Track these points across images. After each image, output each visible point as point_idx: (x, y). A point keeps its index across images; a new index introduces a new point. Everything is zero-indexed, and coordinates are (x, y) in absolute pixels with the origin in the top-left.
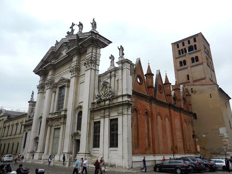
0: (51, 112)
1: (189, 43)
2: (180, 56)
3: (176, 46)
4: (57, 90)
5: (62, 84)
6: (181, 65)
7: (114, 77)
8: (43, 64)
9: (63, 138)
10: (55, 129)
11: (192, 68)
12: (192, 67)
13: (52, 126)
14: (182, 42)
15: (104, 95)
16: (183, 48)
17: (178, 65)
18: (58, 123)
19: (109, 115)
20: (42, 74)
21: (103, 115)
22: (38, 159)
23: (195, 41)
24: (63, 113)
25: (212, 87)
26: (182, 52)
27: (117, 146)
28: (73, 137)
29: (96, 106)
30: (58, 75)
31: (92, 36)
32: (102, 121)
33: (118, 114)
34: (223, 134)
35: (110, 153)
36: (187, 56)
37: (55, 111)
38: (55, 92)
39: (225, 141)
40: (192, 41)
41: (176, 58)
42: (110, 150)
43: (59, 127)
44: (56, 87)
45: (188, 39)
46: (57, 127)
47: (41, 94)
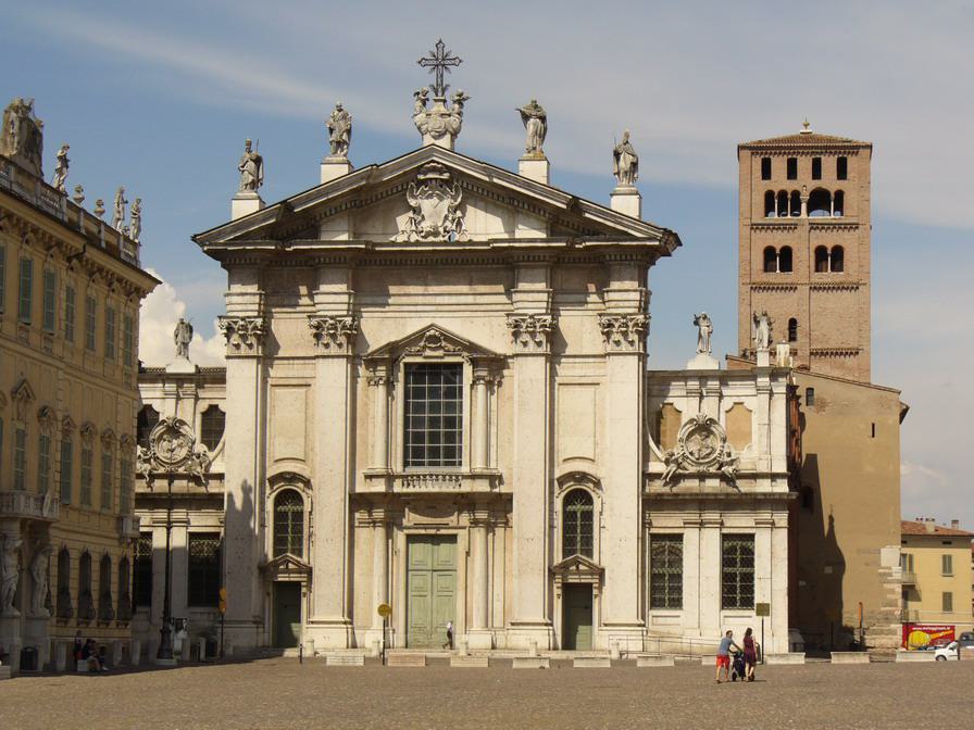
0: (378, 465)
5: (428, 353)
6: (768, 267)
11: (815, 294)
16: (790, 186)
18: (452, 520)
19: (722, 523)
23: (842, 172)
24: (482, 486)
25: (881, 397)
28: (552, 573)
29: (657, 487)
32: (690, 536)
33: (757, 523)
34: (890, 568)
36: (803, 231)
39: (892, 591)
40: (829, 164)
41: (755, 227)
42: (726, 617)
46: (433, 532)
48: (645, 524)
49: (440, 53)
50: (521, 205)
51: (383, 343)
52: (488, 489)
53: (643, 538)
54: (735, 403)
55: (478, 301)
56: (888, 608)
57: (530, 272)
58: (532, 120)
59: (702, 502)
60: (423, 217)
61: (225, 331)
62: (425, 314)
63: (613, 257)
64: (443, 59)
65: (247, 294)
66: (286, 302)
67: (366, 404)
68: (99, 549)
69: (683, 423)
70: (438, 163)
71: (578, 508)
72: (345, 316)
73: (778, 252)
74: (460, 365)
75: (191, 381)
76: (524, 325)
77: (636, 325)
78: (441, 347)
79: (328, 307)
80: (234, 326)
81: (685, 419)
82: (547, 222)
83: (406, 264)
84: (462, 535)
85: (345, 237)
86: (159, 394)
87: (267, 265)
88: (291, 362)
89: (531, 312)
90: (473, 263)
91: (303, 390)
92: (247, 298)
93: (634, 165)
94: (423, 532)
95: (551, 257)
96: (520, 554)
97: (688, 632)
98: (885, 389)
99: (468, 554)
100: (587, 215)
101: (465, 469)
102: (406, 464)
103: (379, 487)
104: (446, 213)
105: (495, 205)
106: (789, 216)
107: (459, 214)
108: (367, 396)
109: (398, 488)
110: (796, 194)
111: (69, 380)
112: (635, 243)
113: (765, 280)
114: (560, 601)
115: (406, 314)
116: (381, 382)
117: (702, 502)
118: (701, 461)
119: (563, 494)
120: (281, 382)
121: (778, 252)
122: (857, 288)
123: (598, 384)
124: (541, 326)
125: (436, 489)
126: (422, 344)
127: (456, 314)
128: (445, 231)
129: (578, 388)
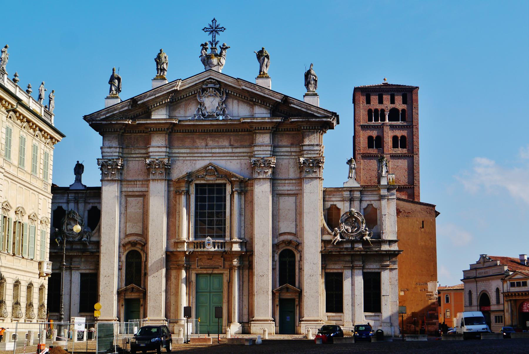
4: (192, 190)
5: (208, 178)
7: (359, 202)
9: (241, 294)
12: (393, 157)
15: (352, 232)
16: (379, 107)
17: (363, 142)
30: (188, 151)
32: (347, 273)
37: (191, 239)
38: (188, 193)
43: (216, 271)
44: (189, 183)
46: (210, 272)
48: (324, 267)
50: (257, 101)
51: (184, 173)
53: (299, 282)
55: (234, 151)
56: (432, 312)
61: (100, 167)
62: (206, 158)
63: (305, 128)
64: (216, 28)
65: (112, 147)
66: (133, 152)
68: (27, 279)
69: (341, 215)
70: (214, 79)
72: (164, 158)
74: (225, 185)
79: (155, 154)
81: (342, 213)
82: (270, 110)
83: (196, 132)
85: (165, 117)
86: (65, 201)
87: (123, 133)
89: (262, 156)
90: (231, 132)
91: (141, 199)
94: (205, 272)
100: (292, 105)
102: (196, 237)
104: (217, 105)
105: (243, 101)
106: (380, 122)
107: (224, 105)
108: (176, 201)
110: (383, 111)
111: (7, 181)
112: (317, 120)
113: (368, 152)
114: (278, 308)
115: (196, 158)
116: (183, 194)
119: (279, 252)
120: (130, 193)
123: (297, 194)
124: (268, 164)
127: (222, 158)
128: (217, 115)
129: (287, 198)
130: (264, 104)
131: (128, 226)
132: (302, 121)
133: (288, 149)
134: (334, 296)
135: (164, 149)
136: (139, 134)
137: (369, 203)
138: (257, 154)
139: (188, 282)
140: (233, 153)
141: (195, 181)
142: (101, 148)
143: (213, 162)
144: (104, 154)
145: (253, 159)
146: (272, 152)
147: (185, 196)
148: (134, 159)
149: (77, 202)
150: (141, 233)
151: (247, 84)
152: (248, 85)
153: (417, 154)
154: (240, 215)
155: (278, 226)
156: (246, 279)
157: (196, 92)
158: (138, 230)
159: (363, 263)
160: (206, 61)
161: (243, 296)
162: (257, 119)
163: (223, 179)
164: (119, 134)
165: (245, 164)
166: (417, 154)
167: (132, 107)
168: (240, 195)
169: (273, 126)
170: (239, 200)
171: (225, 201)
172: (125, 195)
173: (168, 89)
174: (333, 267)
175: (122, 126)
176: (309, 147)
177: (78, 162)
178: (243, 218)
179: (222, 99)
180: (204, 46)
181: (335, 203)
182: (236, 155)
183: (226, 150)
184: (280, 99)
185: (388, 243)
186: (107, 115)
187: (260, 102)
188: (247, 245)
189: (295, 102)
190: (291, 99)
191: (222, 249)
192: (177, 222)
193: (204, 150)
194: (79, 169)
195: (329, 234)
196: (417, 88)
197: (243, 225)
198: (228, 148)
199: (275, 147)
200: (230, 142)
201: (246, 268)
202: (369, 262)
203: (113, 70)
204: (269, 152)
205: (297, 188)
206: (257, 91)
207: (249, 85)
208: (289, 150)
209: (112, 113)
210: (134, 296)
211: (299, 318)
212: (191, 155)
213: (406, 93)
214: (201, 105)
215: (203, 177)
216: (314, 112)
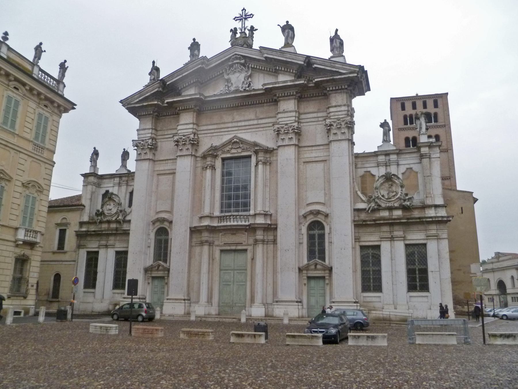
0: (207, 211)
1: (425, 106)
2: (406, 126)
3: (399, 106)
4: (218, 163)
5: (233, 151)
8: (161, 89)
9: (265, 271)
10: (222, 251)
13: (213, 243)
14: (414, 100)
16: (413, 112)
19: (404, 237)
20: (150, 114)
21: (388, 235)
22: (205, 315)
23: (436, 105)
24: (260, 220)
26: (409, 120)
27: (425, 287)
28: (300, 270)
29: (363, 216)
31: (358, 74)
32: (385, 246)
33: (427, 236)
35: (410, 301)
37: (217, 213)
38: (213, 168)
40: (430, 103)
42: (411, 297)
43: (239, 248)
44: (216, 156)
45: (424, 99)
46: (233, 248)
47: (151, 162)
48: (357, 239)
49: (244, 13)
50: (280, 69)
52: (264, 222)
54: (407, 169)
55: (259, 123)
57: (286, 102)
58: (287, 31)
59: (392, 223)
60: (232, 84)
62: (233, 132)
66: (166, 133)
67: (202, 181)
70: (239, 55)
71: (316, 232)
72: (191, 134)
73: (411, 139)
74: (250, 157)
75: (126, 176)
76: (283, 130)
77: (346, 123)
78: (240, 147)
80: (139, 144)
84: (250, 248)
87: (157, 115)
88: (167, 162)
91: (171, 176)
92: (146, 131)
93: (342, 43)
94: (229, 248)
95: (297, 93)
96: (281, 259)
97: (385, 307)
98: (466, 192)
99: (252, 259)
100: (315, 66)
101: (252, 212)
102: (222, 212)
103: (206, 223)
104: (243, 80)
107: (250, 80)
108: (202, 177)
109: (215, 224)
112: (343, 76)
116: (208, 168)
117: (392, 223)
118: (389, 200)
120: (162, 172)
121: (411, 139)
122: (447, 151)
123: (326, 161)
124: (292, 129)
125: (235, 223)
126: (230, 147)
129: (314, 165)
130: (287, 71)
131: (158, 203)
132: (327, 81)
133: (315, 115)
134: (371, 273)
135: (191, 126)
136: (172, 116)
137: (408, 166)
138: (281, 122)
139: (211, 259)
140: (259, 124)
141: (221, 155)
142: (138, 130)
143: (237, 135)
144: (140, 136)
145: (276, 126)
146: (297, 118)
147: (211, 170)
148: (167, 140)
149: (119, 185)
150: (169, 210)
151: (269, 51)
152: (270, 52)
153: (451, 149)
154: (265, 186)
155: (306, 196)
156: (271, 254)
157: (224, 71)
158: (167, 208)
159: (403, 233)
160: (234, 41)
161: (268, 274)
162: (279, 84)
163: (248, 151)
164: (153, 117)
165: (271, 134)
166: (451, 149)
167: (163, 89)
168: (265, 166)
169: (297, 91)
170: (263, 171)
171: (250, 174)
172: (158, 175)
173: (194, 68)
174: (368, 240)
175: (154, 108)
176: (336, 108)
177: (124, 149)
178: (268, 189)
179: (248, 74)
180: (234, 31)
181: (369, 169)
182: (262, 126)
183: (251, 122)
184: (302, 61)
185: (433, 208)
186: (140, 98)
187: (283, 69)
188: (273, 218)
189: (318, 61)
190: (313, 59)
191: (245, 222)
192: (203, 196)
193: (230, 125)
194: (125, 155)
195: (363, 201)
196: (447, 94)
197: (268, 196)
198: (254, 120)
199: (300, 114)
200: (256, 115)
201: (271, 243)
202: (412, 232)
203: (154, 62)
204: (294, 118)
205: (325, 154)
206: (279, 56)
207: (270, 52)
208: (316, 116)
209: (144, 96)
210: (160, 274)
211: (331, 299)
212: (218, 131)
213: (436, 98)
214: (228, 82)
215: (228, 151)
216: (339, 69)
